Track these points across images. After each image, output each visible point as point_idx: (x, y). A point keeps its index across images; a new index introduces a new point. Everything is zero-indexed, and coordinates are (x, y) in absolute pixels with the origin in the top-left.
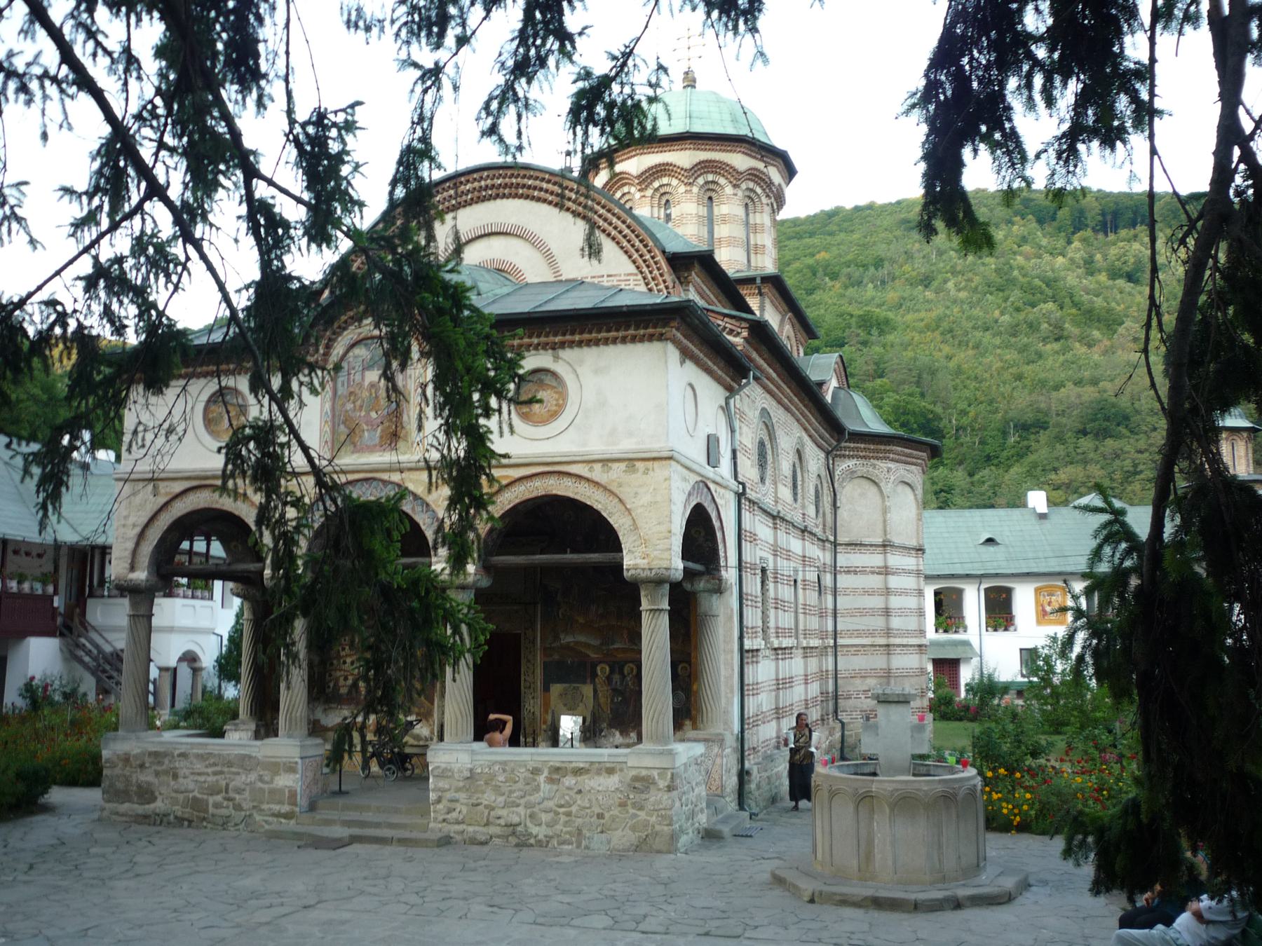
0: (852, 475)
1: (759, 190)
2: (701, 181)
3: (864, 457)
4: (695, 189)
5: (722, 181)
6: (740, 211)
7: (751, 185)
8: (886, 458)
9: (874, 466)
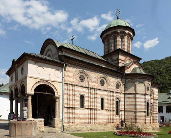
0: (129, 82)
1: (124, 35)
2: (113, 36)
3: (131, 78)
4: (112, 37)
5: (116, 35)
6: (120, 40)
7: (122, 34)
8: (136, 78)
9: (134, 80)
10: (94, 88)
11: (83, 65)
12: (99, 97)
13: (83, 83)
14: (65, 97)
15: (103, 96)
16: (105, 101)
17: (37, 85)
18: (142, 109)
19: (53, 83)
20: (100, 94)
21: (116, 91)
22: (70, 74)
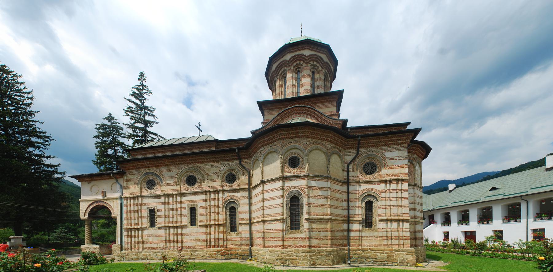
10: (170, 193)
11: (148, 164)
12: (186, 207)
13: (153, 191)
14: (125, 215)
15: (195, 203)
16: (200, 211)
17: (91, 207)
18: (274, 215)
19: (107, 202)
20: (186, 202)
21: (226, 188)
22: (130, 184)
